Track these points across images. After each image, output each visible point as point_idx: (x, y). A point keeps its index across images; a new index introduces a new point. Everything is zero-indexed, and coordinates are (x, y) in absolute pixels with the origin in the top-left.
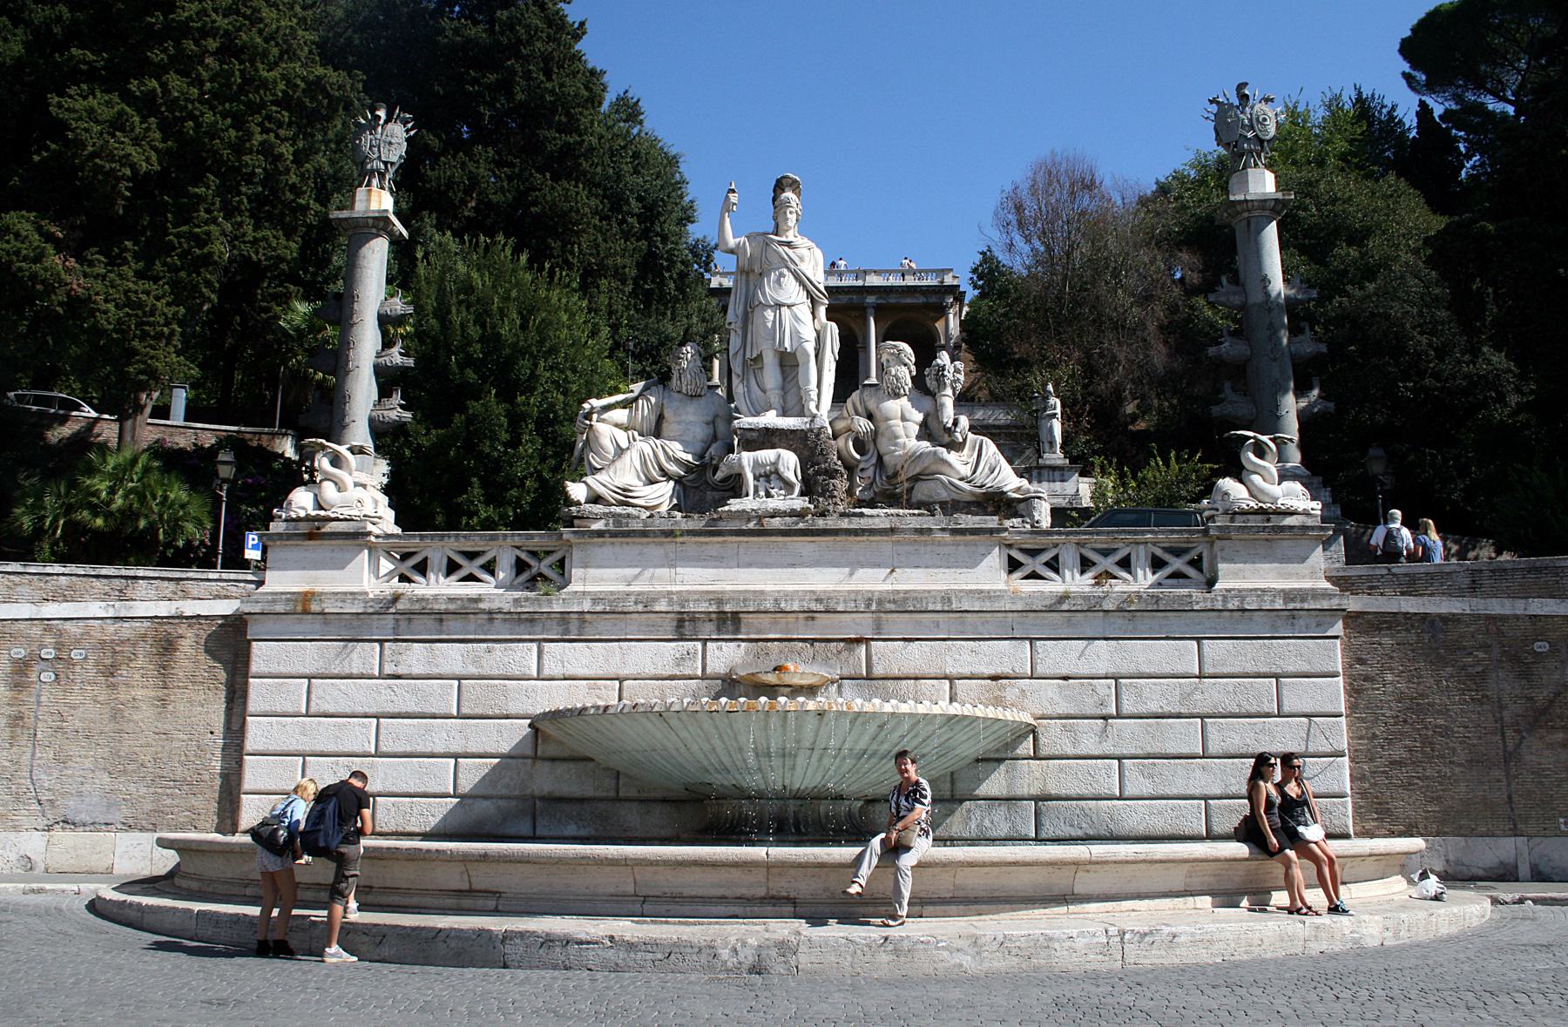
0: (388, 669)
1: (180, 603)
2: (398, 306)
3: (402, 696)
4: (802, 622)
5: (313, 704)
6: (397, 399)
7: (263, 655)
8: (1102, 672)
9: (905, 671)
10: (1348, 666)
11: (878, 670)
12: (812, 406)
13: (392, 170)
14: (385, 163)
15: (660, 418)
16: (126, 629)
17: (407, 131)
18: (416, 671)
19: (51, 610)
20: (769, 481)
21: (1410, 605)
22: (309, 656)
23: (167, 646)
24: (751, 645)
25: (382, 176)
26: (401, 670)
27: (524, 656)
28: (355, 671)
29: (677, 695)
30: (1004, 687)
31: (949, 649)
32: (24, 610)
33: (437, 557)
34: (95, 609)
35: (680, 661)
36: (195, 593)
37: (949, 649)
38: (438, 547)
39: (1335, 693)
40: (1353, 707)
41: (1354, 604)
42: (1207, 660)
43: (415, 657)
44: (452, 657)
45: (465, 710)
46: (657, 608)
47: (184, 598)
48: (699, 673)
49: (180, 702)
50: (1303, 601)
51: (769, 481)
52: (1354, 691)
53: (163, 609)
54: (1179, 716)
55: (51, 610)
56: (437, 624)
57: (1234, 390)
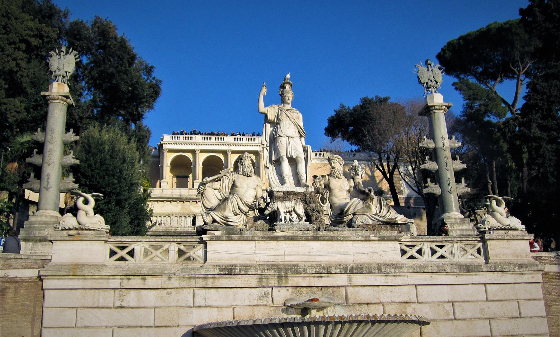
0: (118, 304)
1: (6, 271)
2: (71, 136)
4: (316, 279)
5: (78, 322)
6: (71, 178)
7: (50, 298)
8: (447, 300)
9: (362, 301)
10: (545, 295)
11: (351, 301)
12: (304, 181)
13: (69, 75)
14: (66, 72)
15: (234, 186)
17: (76, 59)
18: (131, 305)
20: (291, 215)
22: (76, 298)
24: (294, 290)
25: (64, 77)
26: (124, 304)
27: (186, 296)
28: (100, 305)
30: (405, 308)
31: (382, 290)
35: (261, 297)
36: (15, 266)
37: (382, 290)
38: (139, 245)
39: (540, 308)
40: (548, 313)
42: (489, 294)
43: (131, 298)
44: (150, 298)
45: (156, 325)
46: (250, 273)
47: (9, 268)
48: (271, 302)
50: (526, 267)
51: (291, 215)
54: (480, 319)
56: (142, 281)
57: (432, 182)
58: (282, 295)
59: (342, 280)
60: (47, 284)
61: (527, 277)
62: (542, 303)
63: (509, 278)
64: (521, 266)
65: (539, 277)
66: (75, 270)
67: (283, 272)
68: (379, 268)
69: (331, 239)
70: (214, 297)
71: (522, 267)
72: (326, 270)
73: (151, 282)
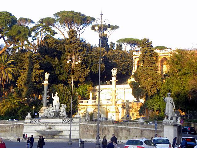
3: (31, 129)
16: (17, 125)
19: (13, 124)
21: (83, 124)
22: (27, 127)
23: (19, 126)
29: (45, 129)
32: (11, 124)
33: (34, 120)
34: (15, 124)
39: (78, 129)
41: (81, 123)
43: (32, 127)
44: (34, 127)
49: (20, 129)
52: (80, 129)
53: (19, 124)
55: (13, 124)
58: (47, 127)
59: (54, 125)
60: (24, 125)
61: (77, 125)
62: (79, 129)
63: (75, 125)
64: (76, 123)
65: (79, 125)
66: (26, 123)
67: (48, 123)
68: (58, 123)
69: (55, 119)
70: (41, 127)
71: (77, 123)
72: (52, 123)
73: (34, 125)
